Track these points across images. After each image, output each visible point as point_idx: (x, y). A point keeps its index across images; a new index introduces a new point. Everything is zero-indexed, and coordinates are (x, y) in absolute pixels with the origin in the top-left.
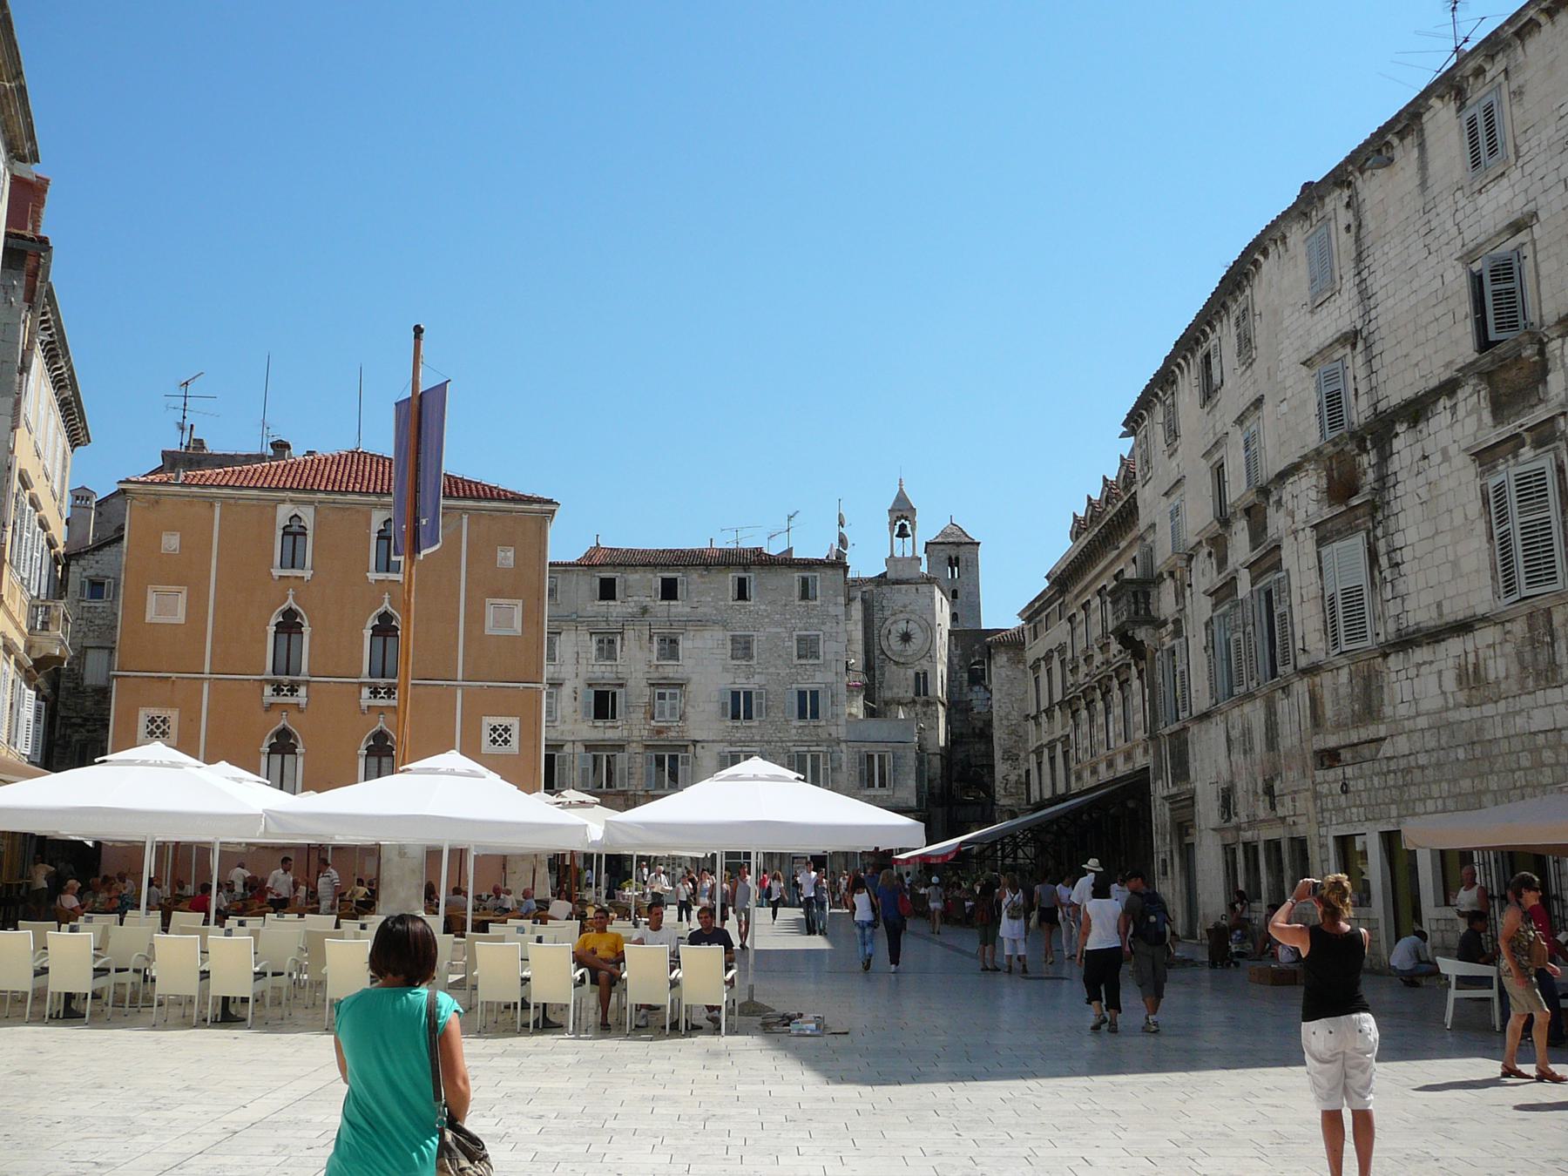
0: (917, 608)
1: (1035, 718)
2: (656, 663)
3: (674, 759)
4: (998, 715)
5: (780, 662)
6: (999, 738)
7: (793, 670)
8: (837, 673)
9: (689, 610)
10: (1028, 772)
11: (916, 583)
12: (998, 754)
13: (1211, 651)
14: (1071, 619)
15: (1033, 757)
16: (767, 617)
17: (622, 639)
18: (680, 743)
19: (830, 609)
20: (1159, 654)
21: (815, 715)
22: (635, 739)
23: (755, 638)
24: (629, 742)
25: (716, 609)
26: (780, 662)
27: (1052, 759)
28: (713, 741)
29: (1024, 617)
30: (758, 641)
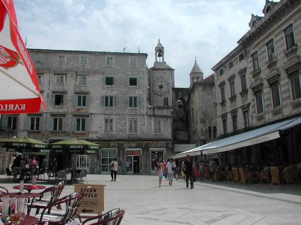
0: (165, 78)
2: (78, 85)
3: (84, 121)
5: (123, 86)
6: (199, 116)
8: (143, 91)
9: (90, 67)
16: (119, 71)
17: (66, 77)
18: (86, 114)
19: (141, 69)
21: (135, 105)
22: (69, 112)
24: (67, 114)
25: (100, 67)
26: (123, 86)
28: (98, 114)
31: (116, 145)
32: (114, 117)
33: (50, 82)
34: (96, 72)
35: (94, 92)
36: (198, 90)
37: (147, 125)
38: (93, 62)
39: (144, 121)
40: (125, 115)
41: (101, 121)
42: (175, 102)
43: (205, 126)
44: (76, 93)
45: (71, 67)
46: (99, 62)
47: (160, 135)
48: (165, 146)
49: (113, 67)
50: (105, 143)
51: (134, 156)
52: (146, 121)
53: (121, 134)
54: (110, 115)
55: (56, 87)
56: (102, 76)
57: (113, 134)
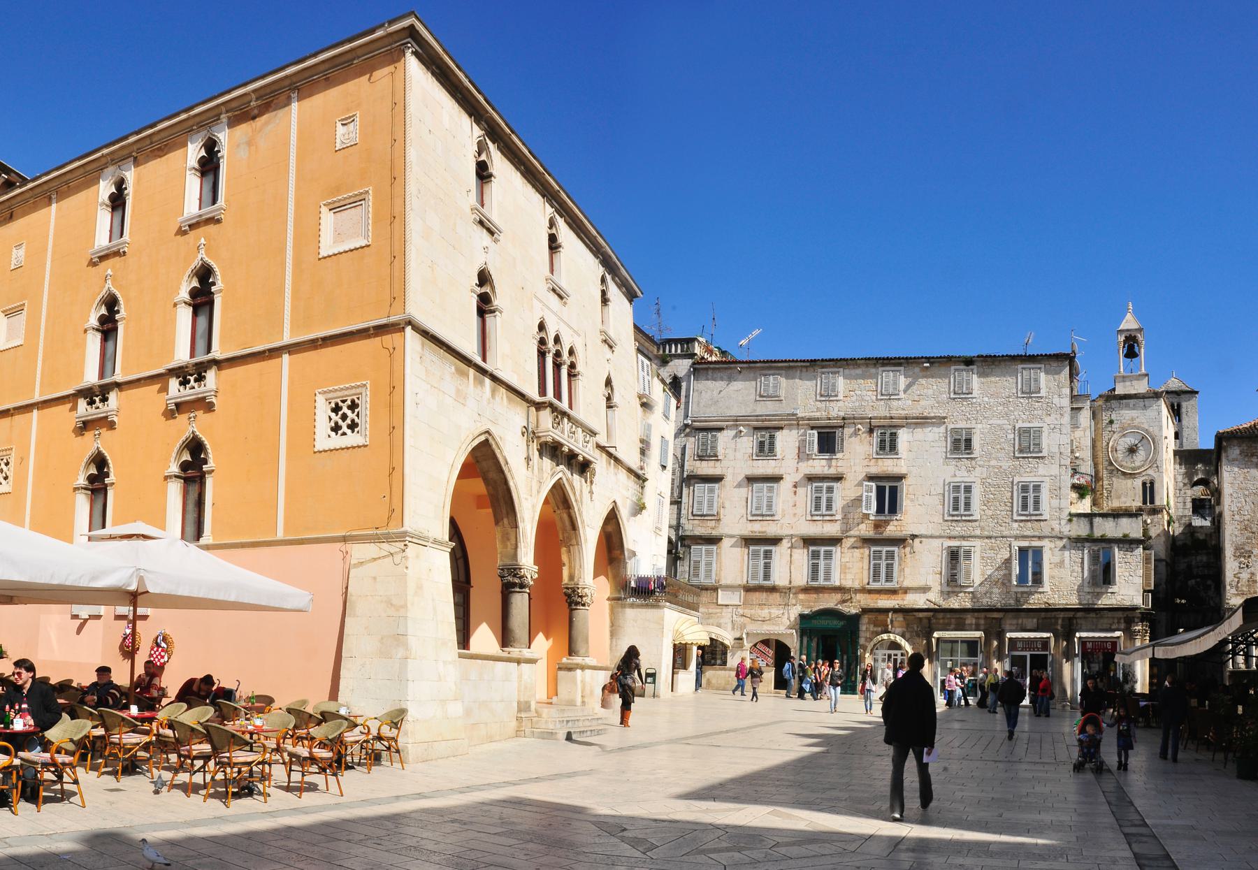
5: (1001, 455)
23: (978, 432)
25: (937, 403)
26: (1001, 455)
28: (931, 537)
31: (982, 622)
33: (801, 451)
34: (922, 421)
36: (1230, 458)
42: (1185, 493)
44: (871, 478)
50: (951, 618)
51: (1031, 655)
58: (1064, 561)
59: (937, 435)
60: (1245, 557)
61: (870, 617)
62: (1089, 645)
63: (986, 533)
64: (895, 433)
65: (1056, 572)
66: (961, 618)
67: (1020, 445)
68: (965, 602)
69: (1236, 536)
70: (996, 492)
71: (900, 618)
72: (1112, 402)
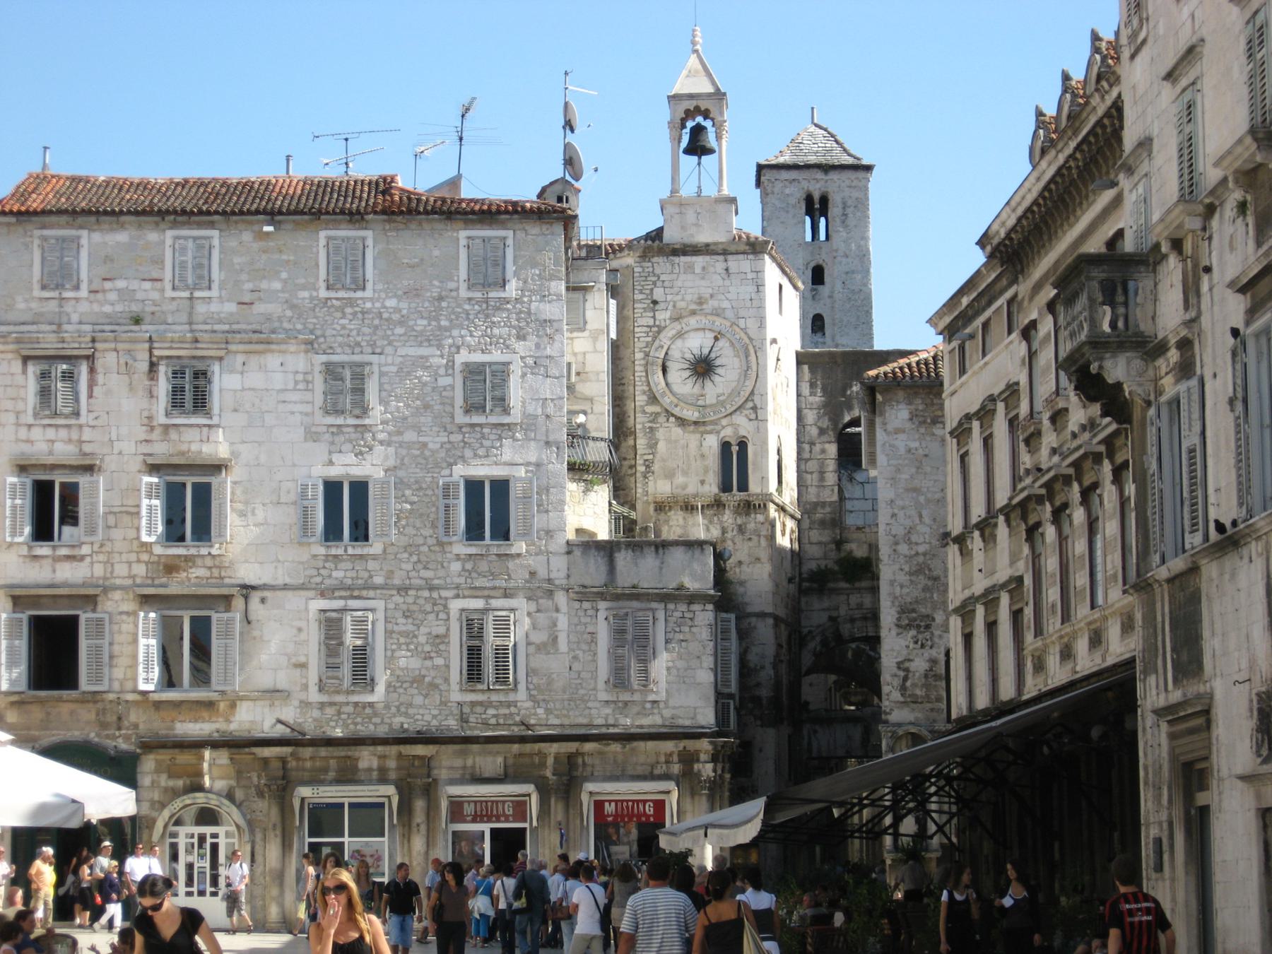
0: (726, 304)
1: (960, 540)
2: (162, 420)
4: (889, 533)
5: (426, 419)
6: (892, 583)
7: (456, 438)
9: (231, 307)
10: (947, 654)
11: (725, 253)
12: (888, 616)
13: (1239, 407)
14: (1028, 332)
15: (955, 623)
16: (401, 323)
17: (92, 370)
18: (215, 591)
20: (1152, 412)
21: (502, 532)
22: (118, 582)
23: (376, 369)
25: (293, 307)
26: (426, 419)
27: (991, 627)
28: (286, 587)
29: (942, 325)
30: (382, 374)
31: (392, 764)
32: (379, 604)
35: (257, 458)
36: (890, 427)
37: (571, 650)
38: (244, 277)
39: (555, 625)
40: (437, 588)
41: (300, 630)
43: (923, 646)
45: (119, 308)
46: (284, 275)
47: (648, 706)
48: (676, 769)
49: (368, 305)
50: (326, 758)
51: (492, 830)
52: (563, 622)
53: (418, 700)
54: (356, 593)
55: (37, 433)
56: (298, 361)
57: (371, 705)
58: (557, 637)
59: (291, 376)
60: (918, 627)
61: (159, 757)
62: (609, 809)
63: (397, 582)
64: (204, 373)
65: (539, 661)
66: (349, 757)
67: (465, 400)
68: (356, 724)
69: (902, 586)
70: (416, 499)
71: (223, 757)
72: (655, 259)
